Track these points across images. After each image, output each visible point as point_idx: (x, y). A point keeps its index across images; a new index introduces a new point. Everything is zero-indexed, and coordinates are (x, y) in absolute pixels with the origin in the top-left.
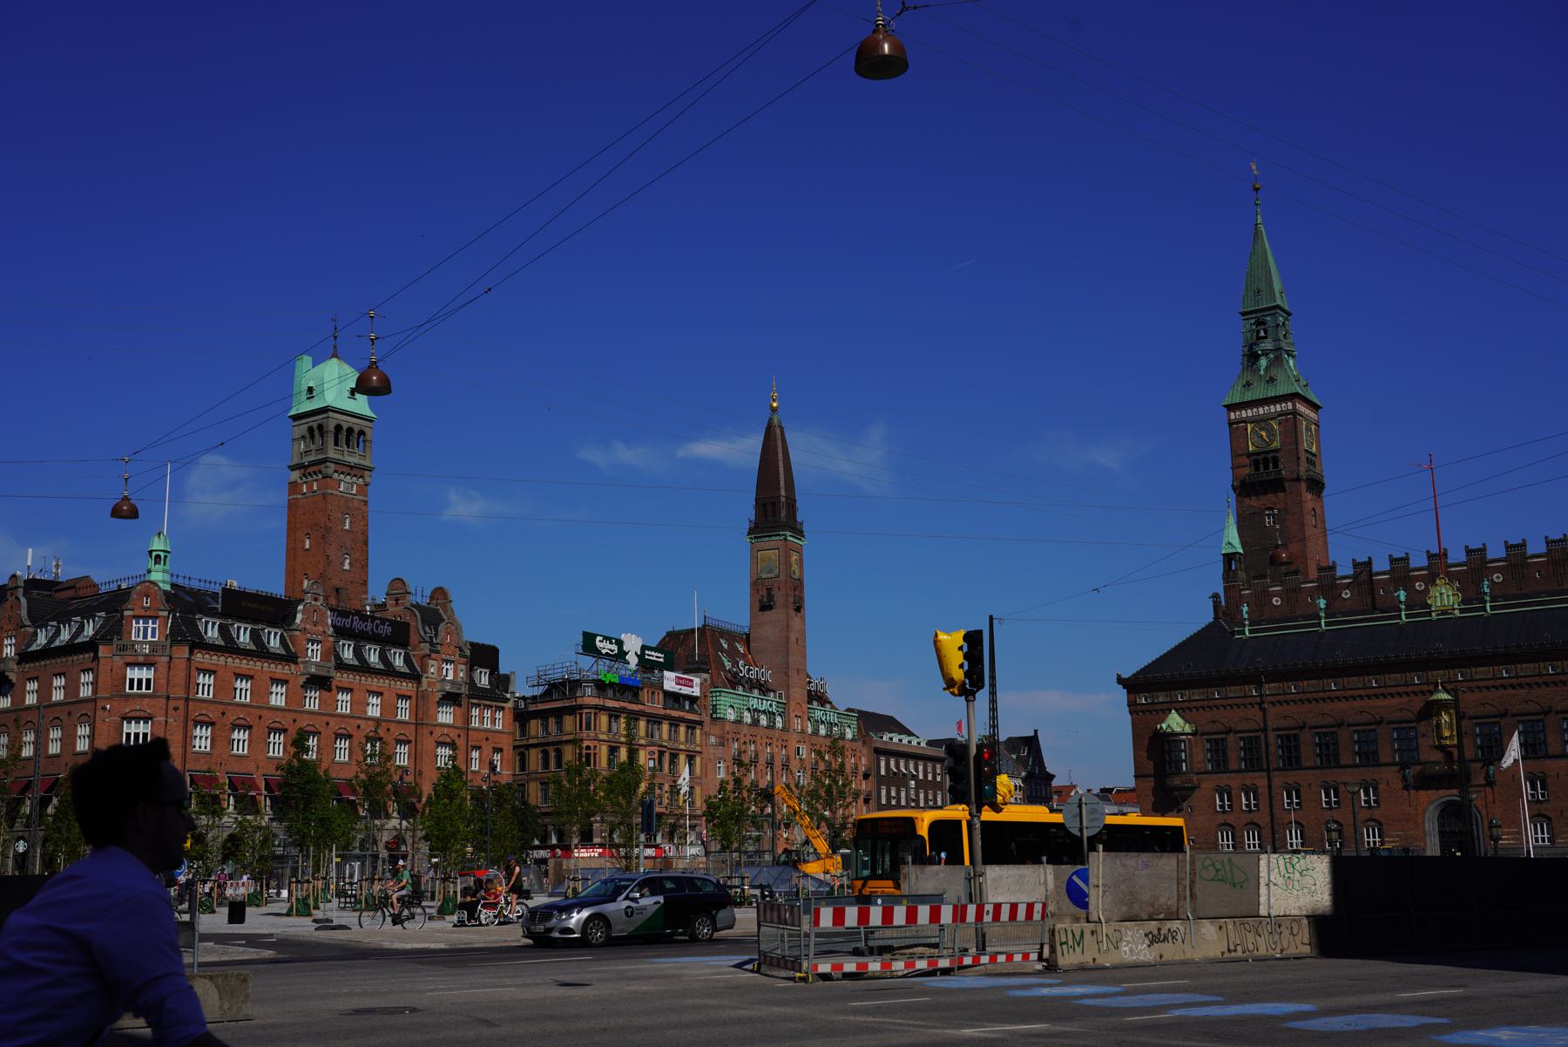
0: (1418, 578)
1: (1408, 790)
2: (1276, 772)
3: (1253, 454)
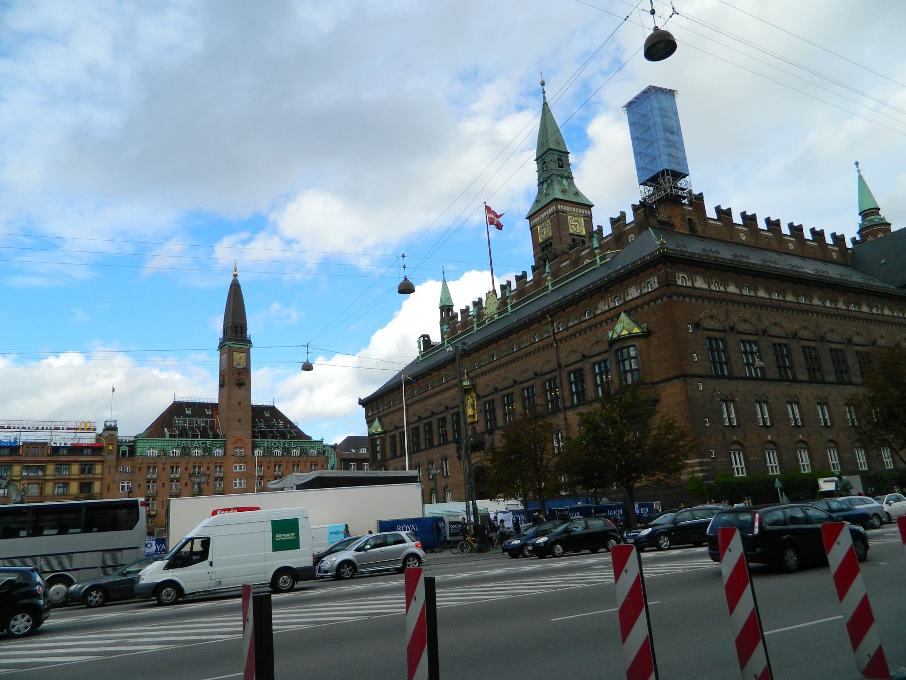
3: (542, 243)
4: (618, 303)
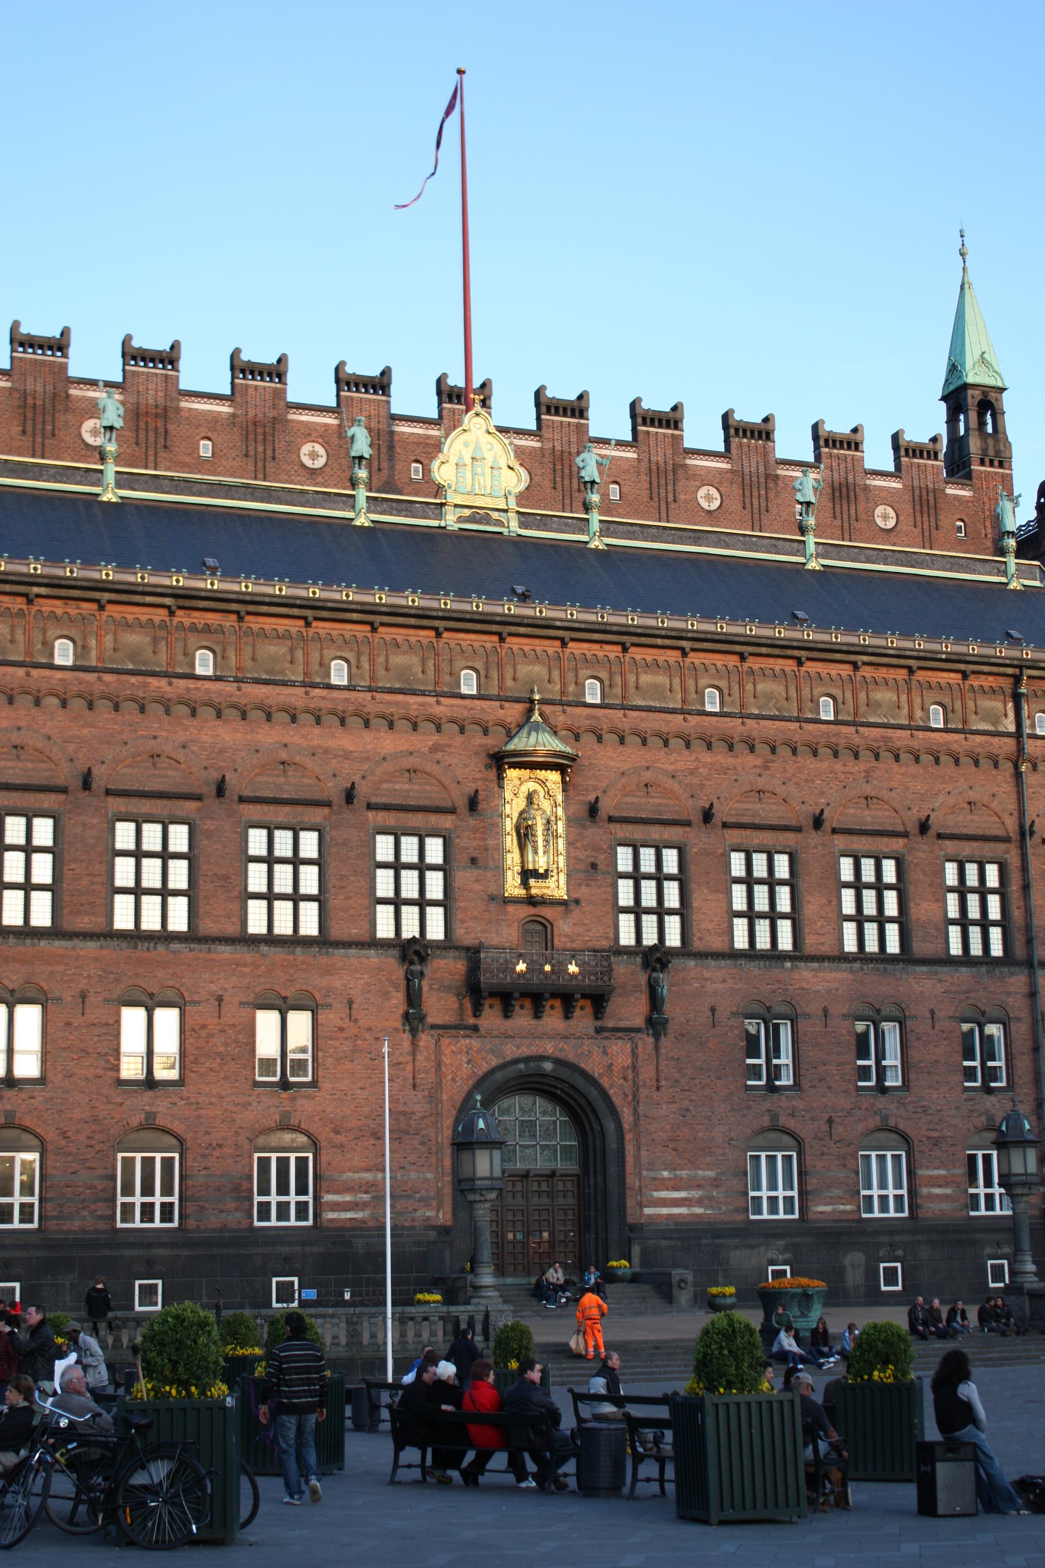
0: (310, 433)
1: (414, 1032)
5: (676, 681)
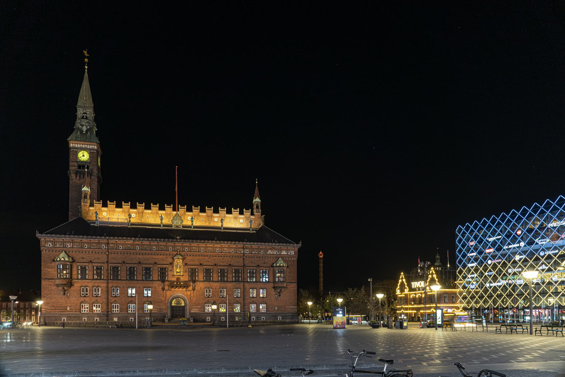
2: (109, 281)
4: (276, 253)
5: (197, 248)
